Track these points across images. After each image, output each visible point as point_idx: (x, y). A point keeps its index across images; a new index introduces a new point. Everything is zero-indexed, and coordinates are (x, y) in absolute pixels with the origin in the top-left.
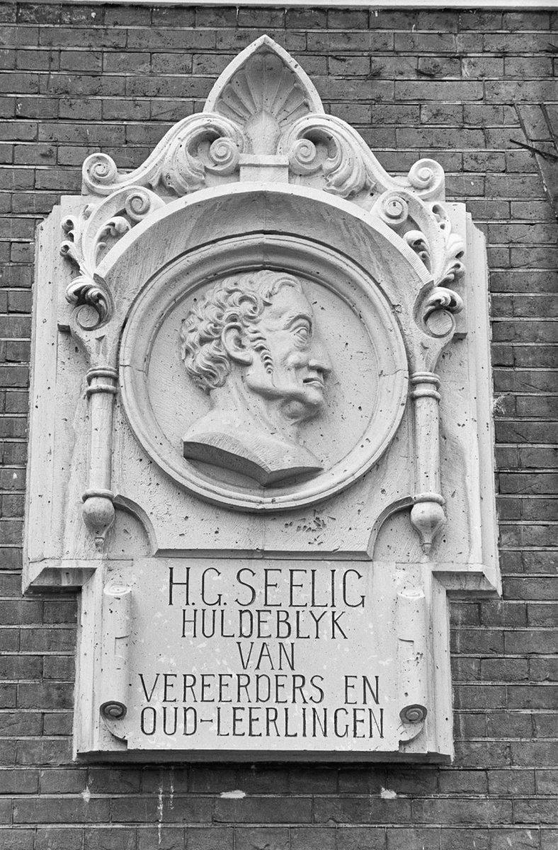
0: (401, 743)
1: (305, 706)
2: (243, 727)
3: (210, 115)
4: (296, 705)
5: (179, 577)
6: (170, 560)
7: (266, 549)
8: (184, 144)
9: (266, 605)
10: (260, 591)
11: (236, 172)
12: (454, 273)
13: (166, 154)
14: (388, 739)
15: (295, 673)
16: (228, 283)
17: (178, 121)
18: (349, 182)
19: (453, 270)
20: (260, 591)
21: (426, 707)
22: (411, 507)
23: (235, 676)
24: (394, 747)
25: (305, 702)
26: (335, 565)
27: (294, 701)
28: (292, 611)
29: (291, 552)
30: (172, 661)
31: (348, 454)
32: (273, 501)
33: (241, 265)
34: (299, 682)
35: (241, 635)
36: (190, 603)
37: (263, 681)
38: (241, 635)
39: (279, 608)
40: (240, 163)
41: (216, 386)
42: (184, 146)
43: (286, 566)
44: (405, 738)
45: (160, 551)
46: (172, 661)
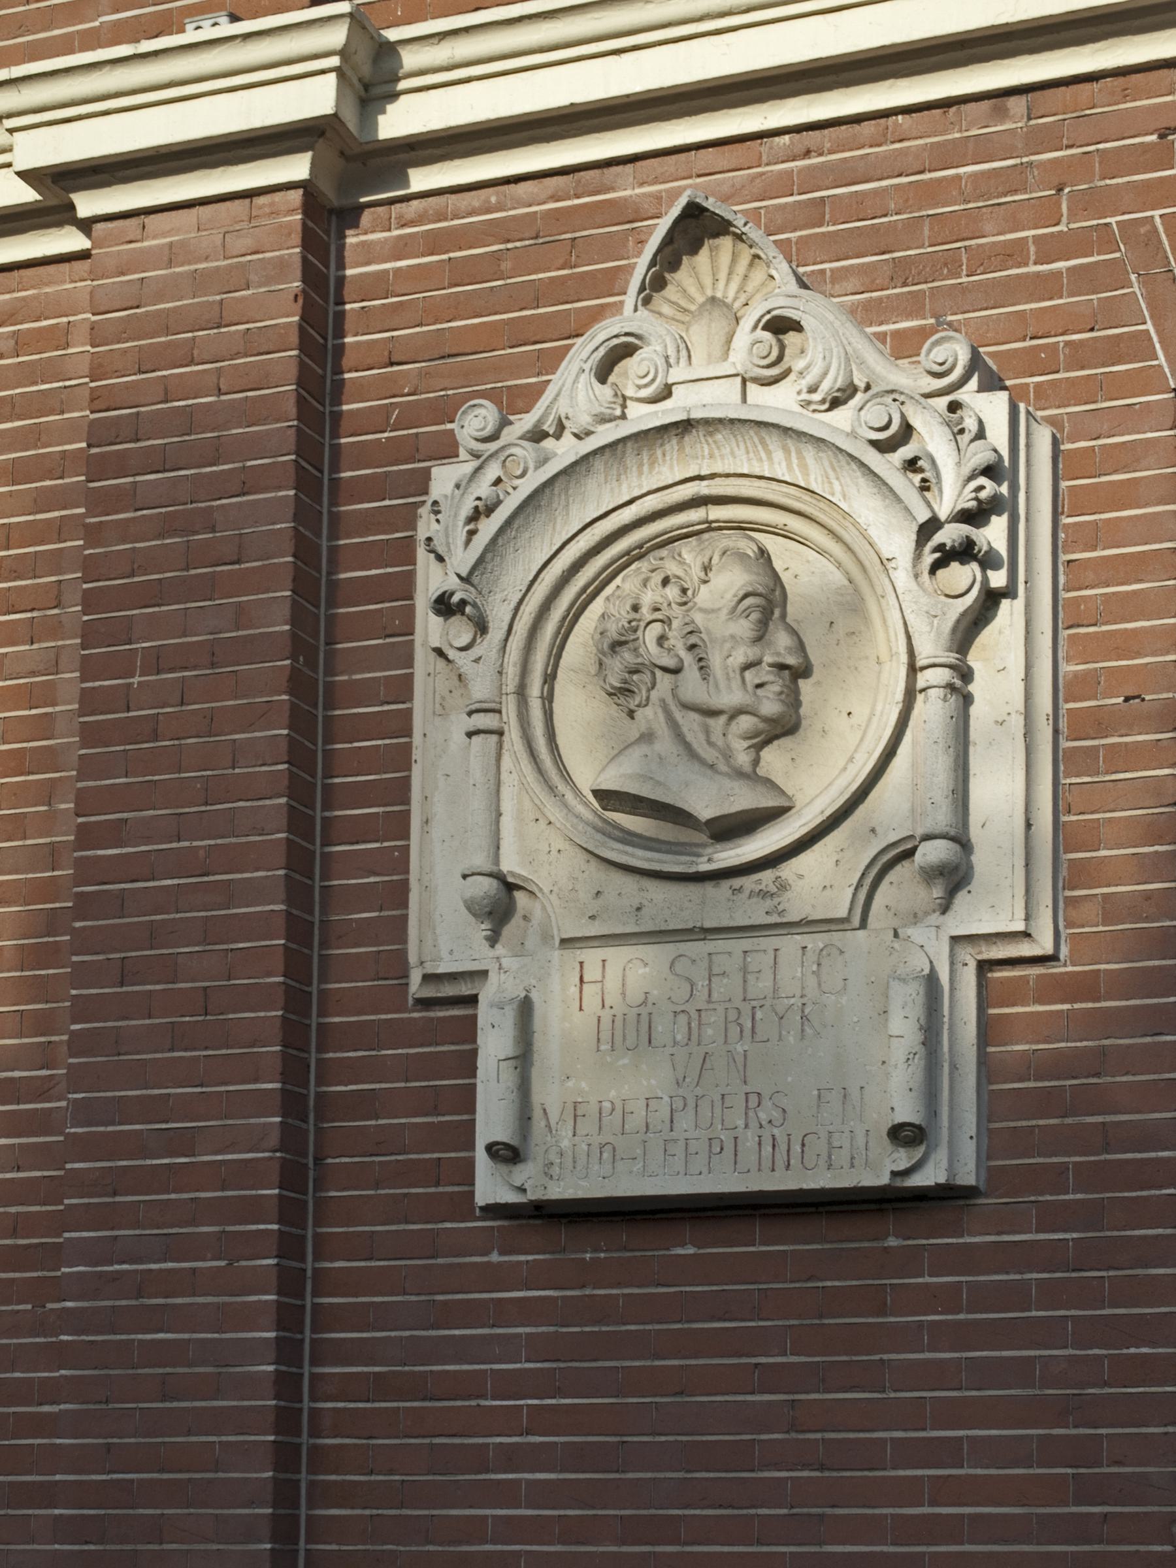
0: (894, 1174)
1: (760, 1132)
2: (678, 1163)
3: (630, 316)
4: (749, 1133)
5: (592, 973)
6: (578, 952)
7: (708, 924)
8: (587, 366)
9: (709, 1002)
10: (701, 984)
11: (666, 392)
12: (976, 499)
13: (563, 385)
14: (878, 1169)
15: (748, 1089)
16: (643, 566)
17: (582, 335)
18: (825, 386)
19: (973, 495)
20: (701, 984)
21: (924, 1125)
22: (914, 849)
23: (666, 1099)
24: (884, 1180)
25: (761, 1126)
26: (806, 940)
27: (746, 1126)
28: (746, 1009)
29: (456, 973)
30: (583, 1084)
31: (826, 788)
32: (709, 860)
33: (678, 529)
34: (753, 1100)
35: (675, 1043)
36: (607, 1004)
37: (705, 1106)
38: (675, 1043)
39: (728, 1005)
40: (670, 381)
41: (638, 706)
42: (587, 371)
43: (737, 945)
44: (902, 1165)
45: (563, 941)
46: (583, 1084)
